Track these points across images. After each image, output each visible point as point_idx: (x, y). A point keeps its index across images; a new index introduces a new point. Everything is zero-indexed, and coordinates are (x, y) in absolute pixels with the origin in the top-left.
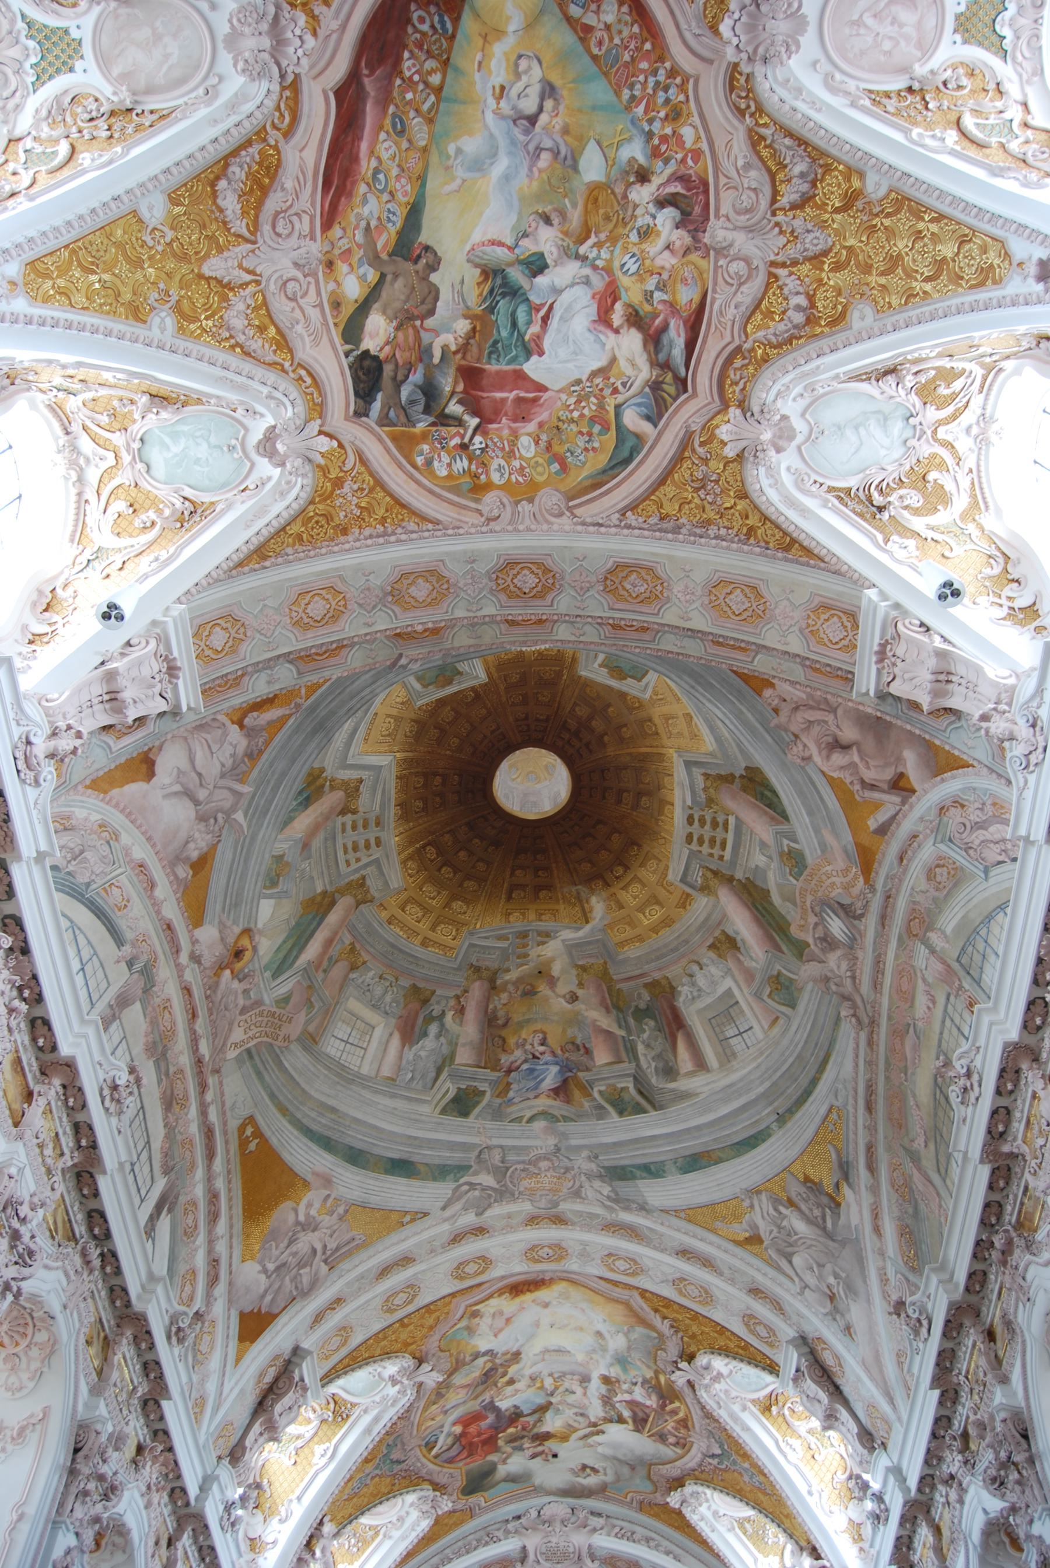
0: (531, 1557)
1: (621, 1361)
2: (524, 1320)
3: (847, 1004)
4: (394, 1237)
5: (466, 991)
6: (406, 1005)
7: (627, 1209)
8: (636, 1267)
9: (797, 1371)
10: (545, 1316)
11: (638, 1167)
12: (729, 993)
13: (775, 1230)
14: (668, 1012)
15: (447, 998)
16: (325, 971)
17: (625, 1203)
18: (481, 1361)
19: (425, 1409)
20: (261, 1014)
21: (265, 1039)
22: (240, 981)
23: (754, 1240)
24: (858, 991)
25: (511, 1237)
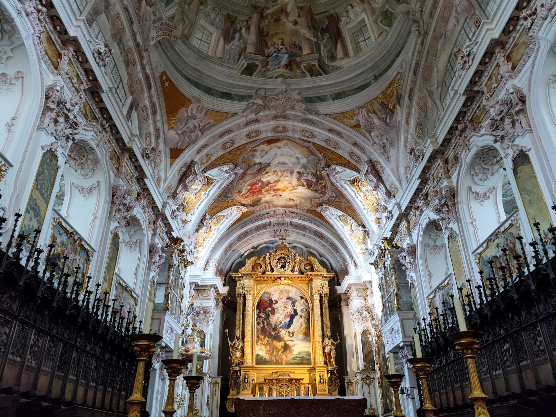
0: (272, 224)
1: (305, 167)
2: (272, 153)
3: (416, 24)
4: (225, 123)
5: (251, 18)
6: (225, 24)
7: (311, 114)
8: (312, 135)
9: (367, 171)
10: (279, 151)
11: (317, 98)
12: (363, 20)
13: (366, 122)
14: (335, 30)
15: (242, 21)
16: (189, 4)
17: (310, 112)
18: (257, 166)
19: (238, 181)
20: (162, 24)
21: (166, 36)
22: (151, 7)
23: (357, 126)
24: (422, 18)
25: (268, 124)
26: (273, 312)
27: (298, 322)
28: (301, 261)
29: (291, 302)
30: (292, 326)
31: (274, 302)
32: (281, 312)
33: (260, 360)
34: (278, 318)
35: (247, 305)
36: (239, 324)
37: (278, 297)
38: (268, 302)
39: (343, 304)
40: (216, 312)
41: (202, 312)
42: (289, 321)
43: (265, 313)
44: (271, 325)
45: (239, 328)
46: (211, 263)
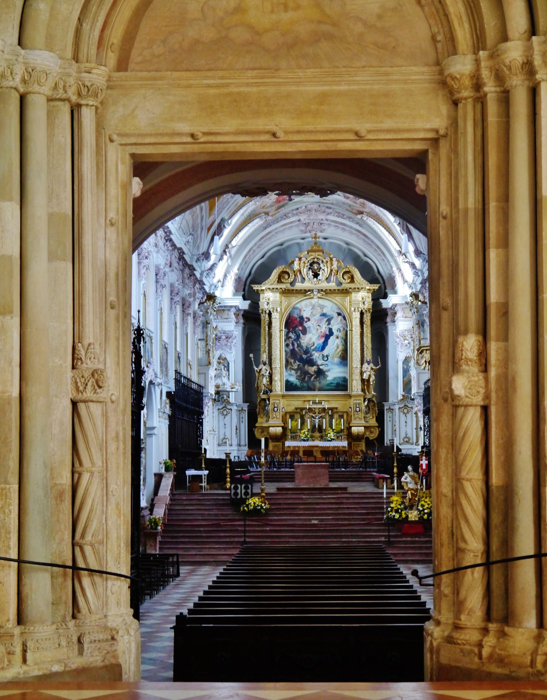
26: (304, 332)
27: (334, 344)
28: (339, 268)
29: (326, 319)
30: (327, 348)
31: (306, 320)
32: (314, 331)
33: (289, 386)
34: (311, 339)
35: (273, 325)
36: (264, 345)
37: (310, 313)
38: (298, 319)
39: (389, 320)
40: (237, 333)
41: (224, 337)
42: (324, 342)
43: (295, 333)
44: (302, 347)
45: (265, 352)
46: (229, 277)
